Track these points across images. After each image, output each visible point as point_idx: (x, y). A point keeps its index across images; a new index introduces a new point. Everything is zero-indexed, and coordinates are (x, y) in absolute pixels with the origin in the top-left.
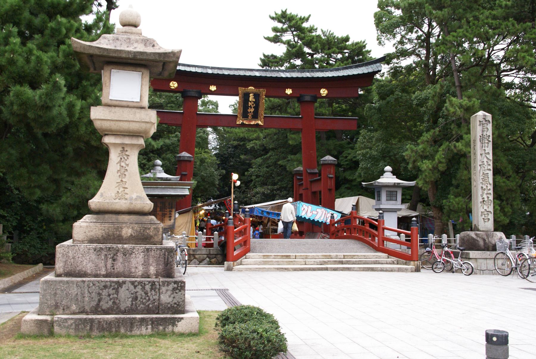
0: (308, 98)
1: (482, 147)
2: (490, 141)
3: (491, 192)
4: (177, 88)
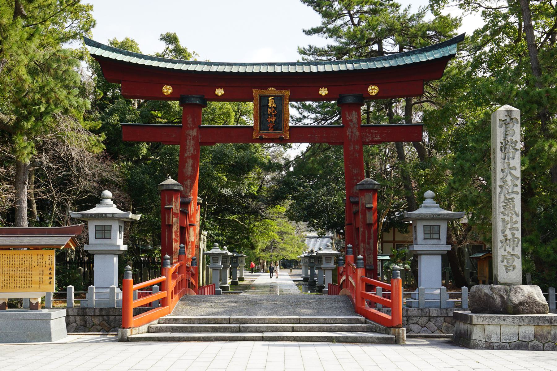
1: (505, 159)
2: (517, 150)
3: (519, 225)
4: (172, 93)
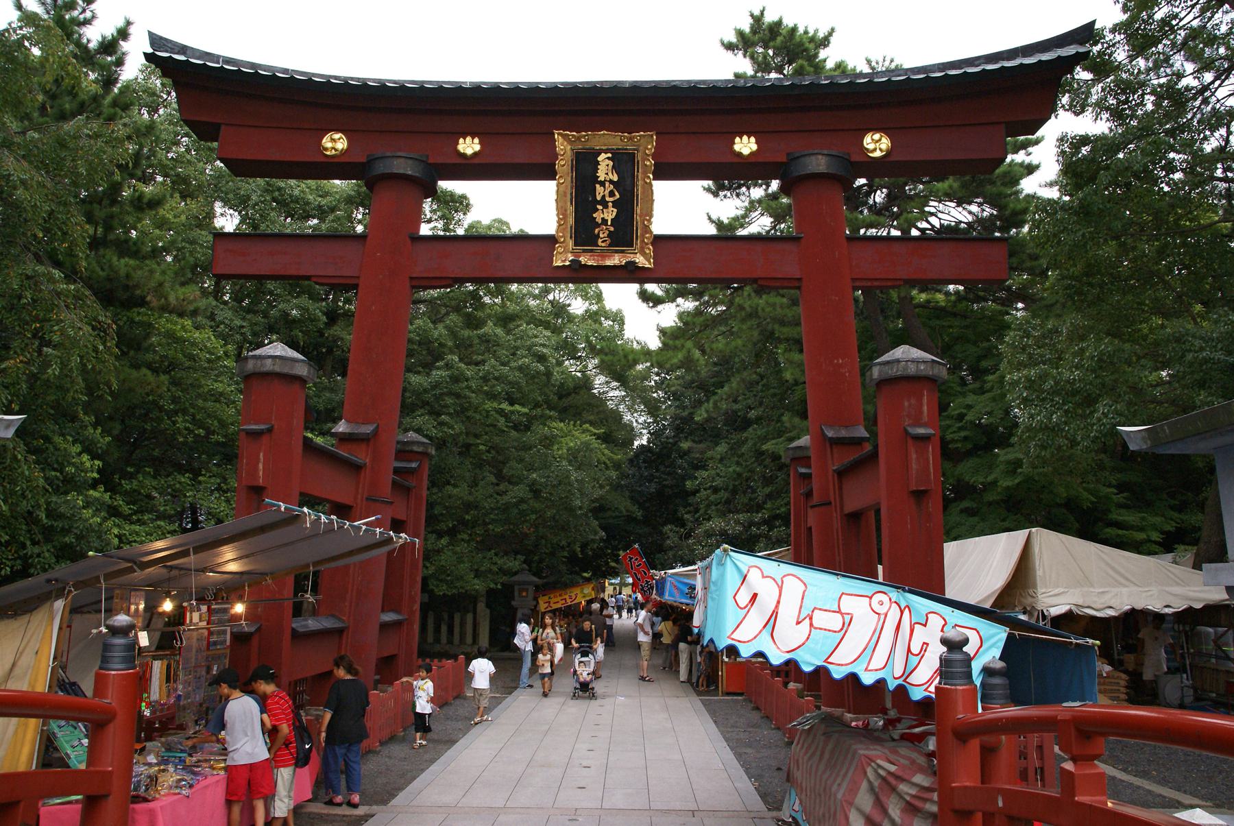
0: (819, 164)
